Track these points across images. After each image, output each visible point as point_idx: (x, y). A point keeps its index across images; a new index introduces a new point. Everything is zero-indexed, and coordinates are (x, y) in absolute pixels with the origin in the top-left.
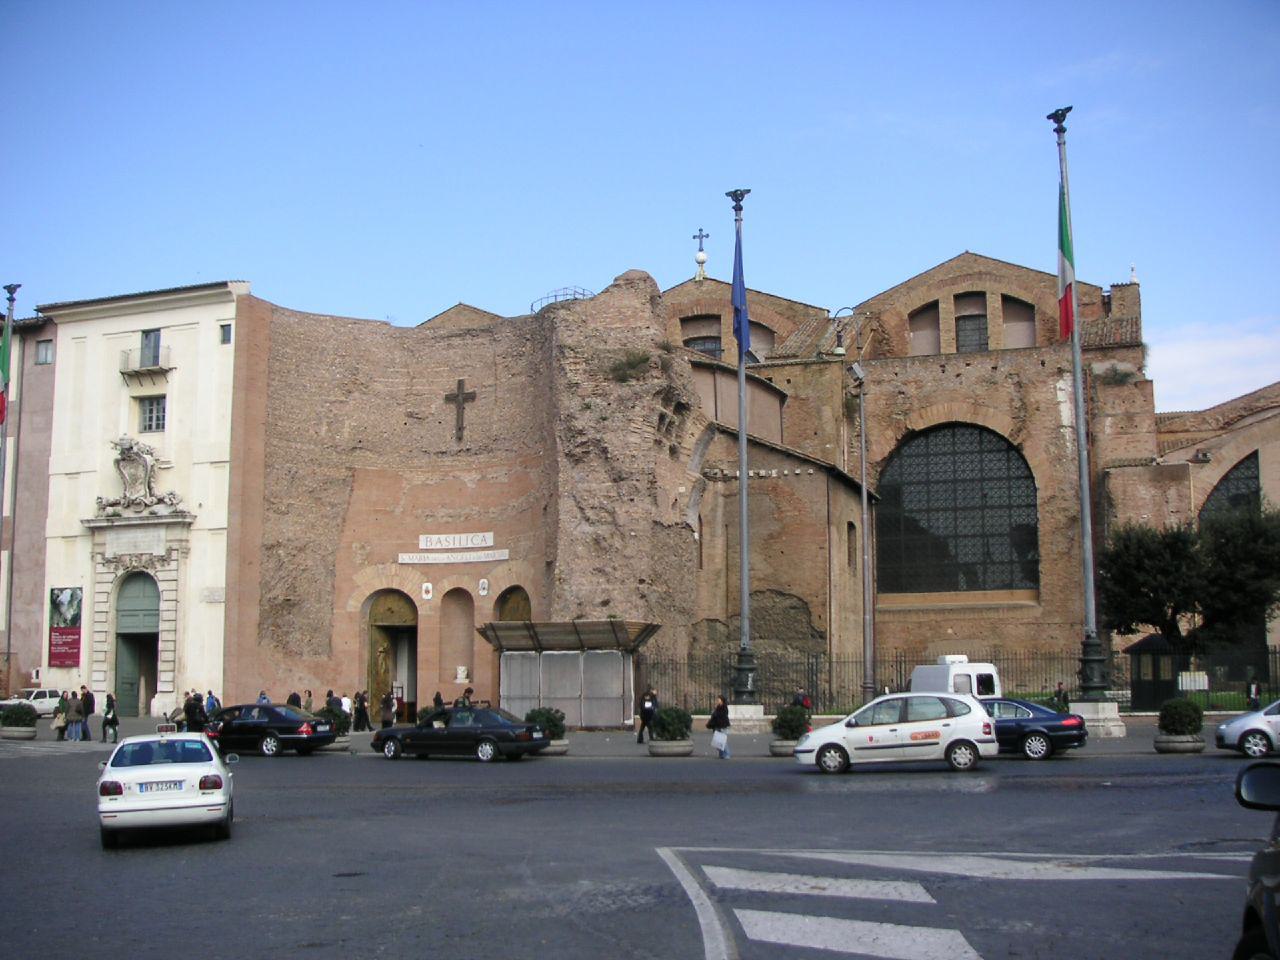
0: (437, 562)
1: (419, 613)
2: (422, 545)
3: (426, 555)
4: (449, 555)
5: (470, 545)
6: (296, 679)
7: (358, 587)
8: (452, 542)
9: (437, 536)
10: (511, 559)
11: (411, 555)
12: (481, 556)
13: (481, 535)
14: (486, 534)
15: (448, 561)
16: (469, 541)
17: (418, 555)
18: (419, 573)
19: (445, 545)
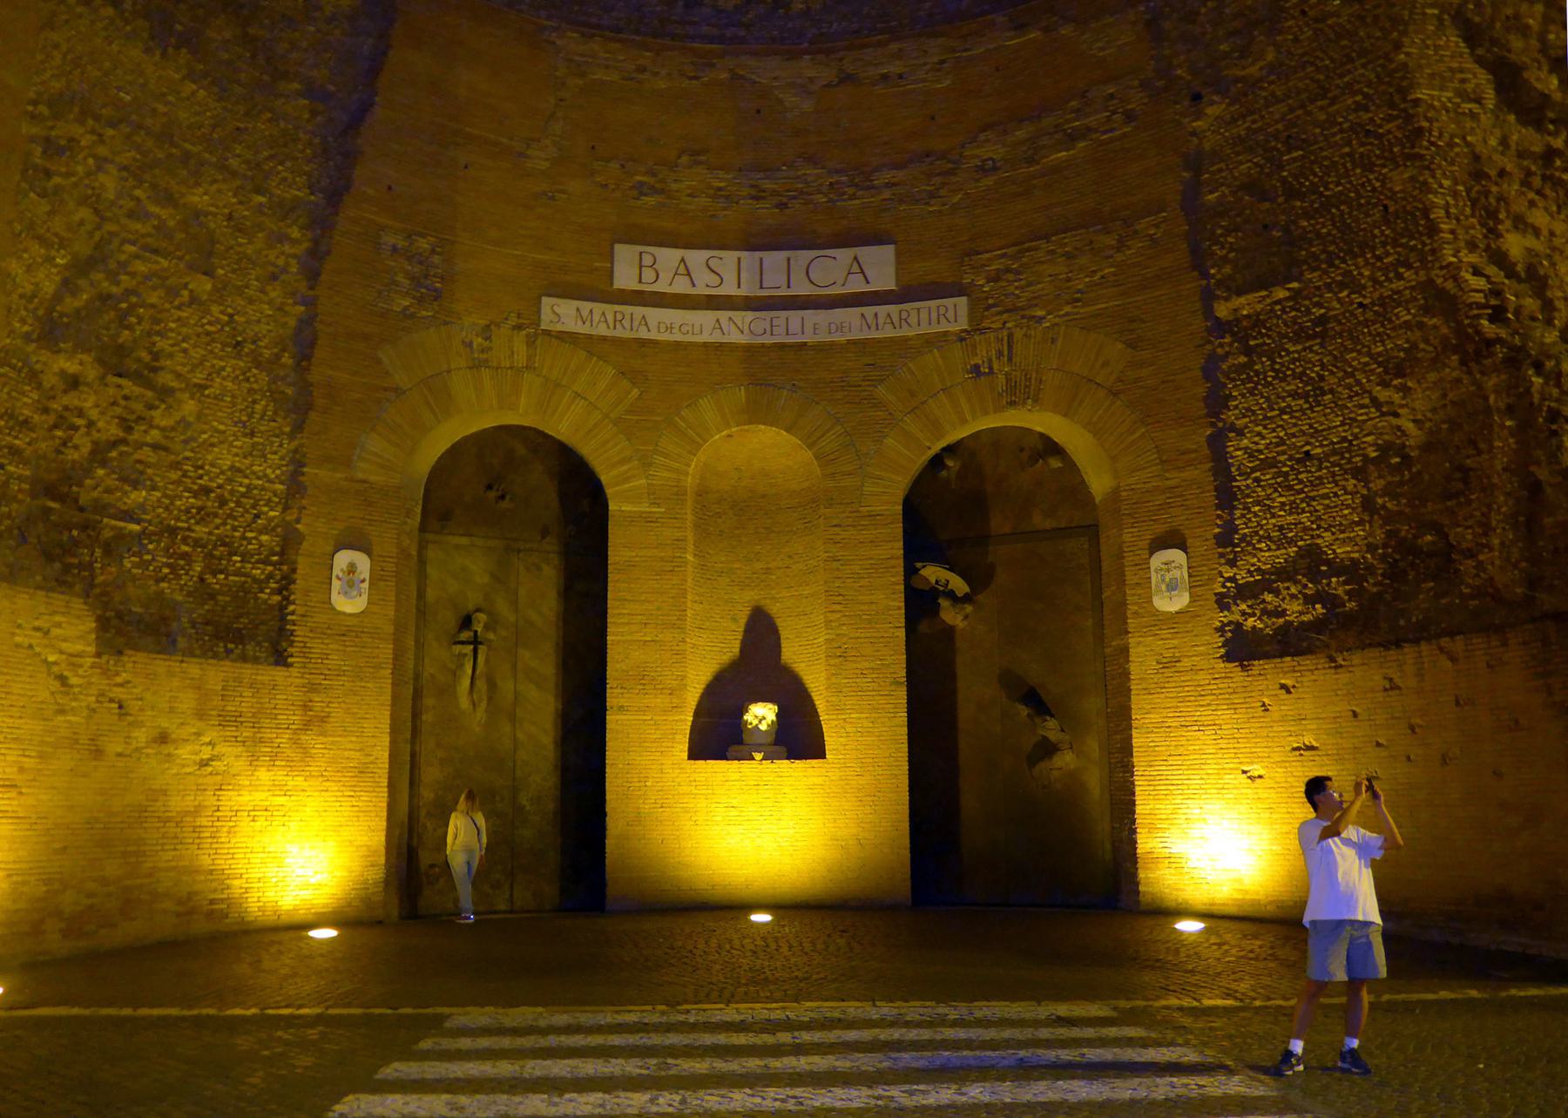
0: (678, 337)
1: (612, 507)
2: (625, 278)
3: (639, 311)
4: (724, 315)
5: (802, 289)
6: (141, 736)
7: (398, 391)
8: (730, 276)
9: (677, 254)
10: (976, 328)
11: (586, 306)
12: (851, 324)
13: (844, 255)
14: (867, 253)
15: (717, 337)
16: (798, 275)
17: (610, 309)
18: (611, 371)
19: (704, 285)
